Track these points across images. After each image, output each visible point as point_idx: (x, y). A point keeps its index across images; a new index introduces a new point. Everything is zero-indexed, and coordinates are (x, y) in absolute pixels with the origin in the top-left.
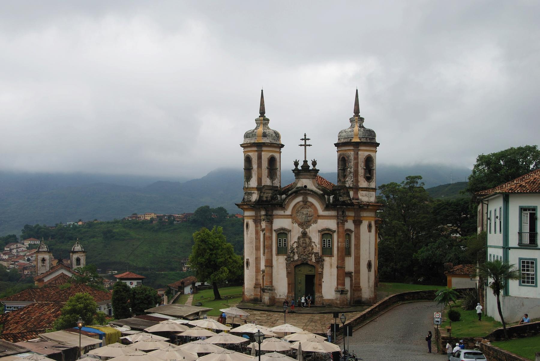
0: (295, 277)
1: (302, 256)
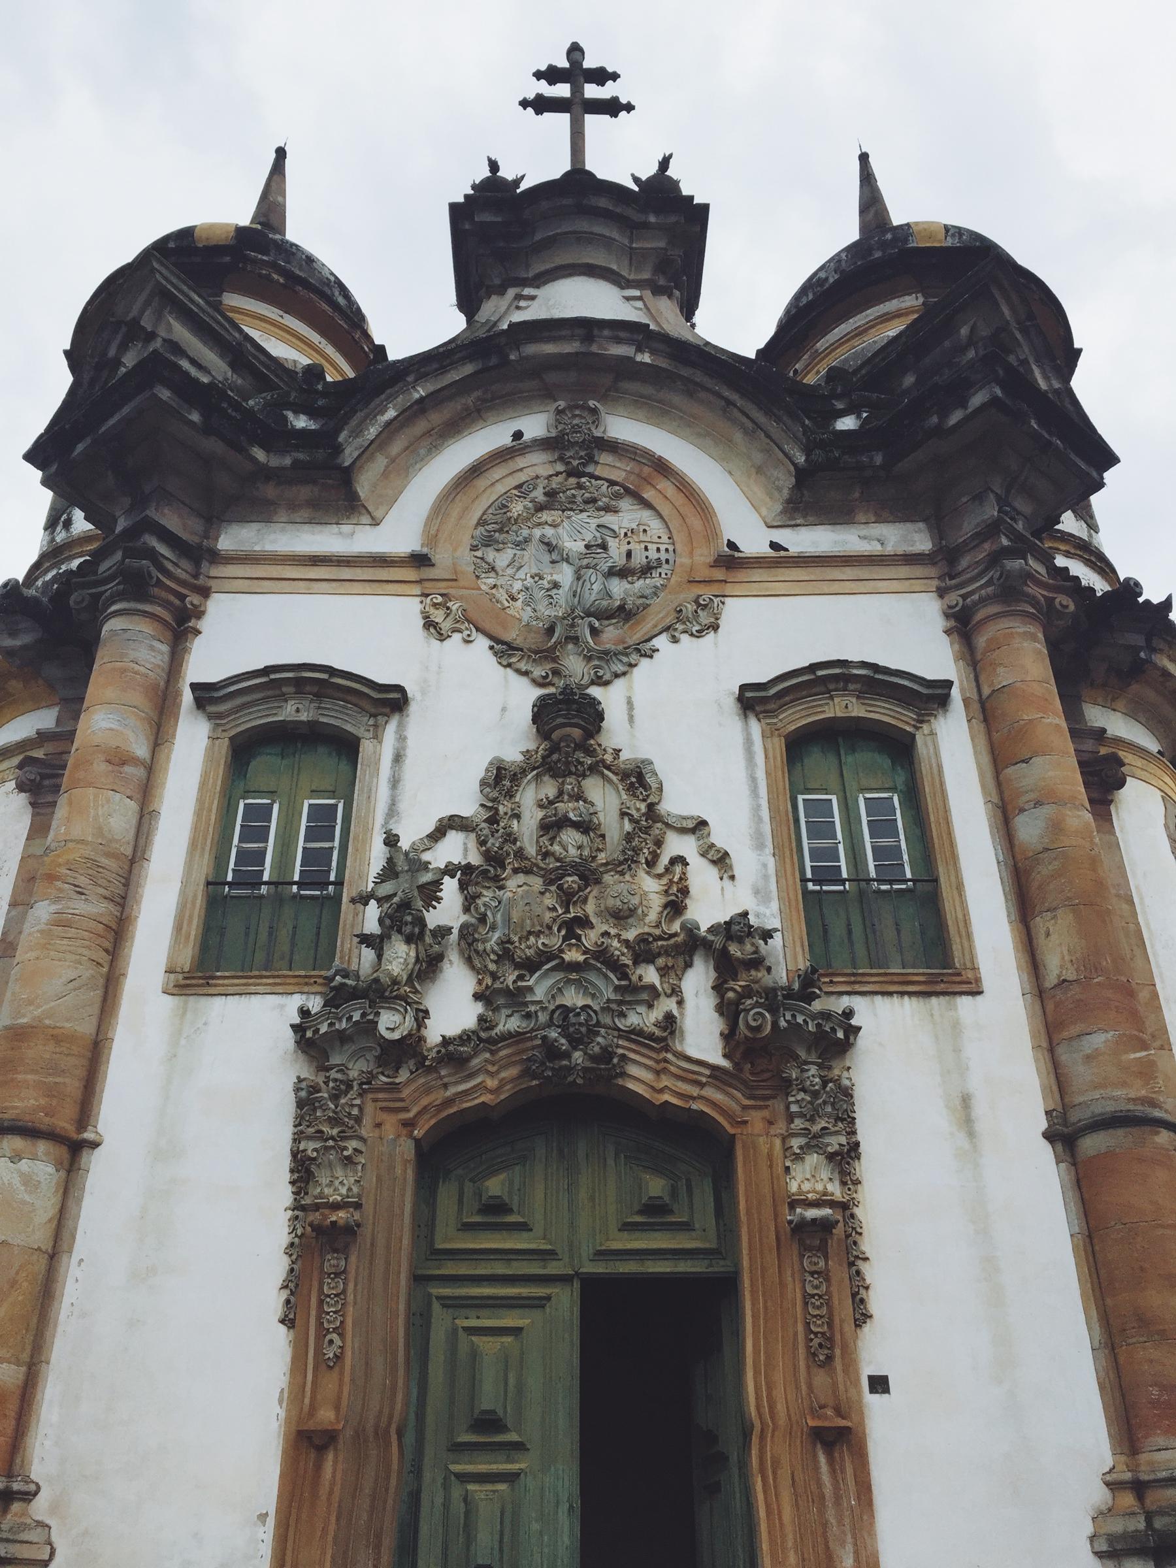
0: (419, 1322)
1: (540, 987)
